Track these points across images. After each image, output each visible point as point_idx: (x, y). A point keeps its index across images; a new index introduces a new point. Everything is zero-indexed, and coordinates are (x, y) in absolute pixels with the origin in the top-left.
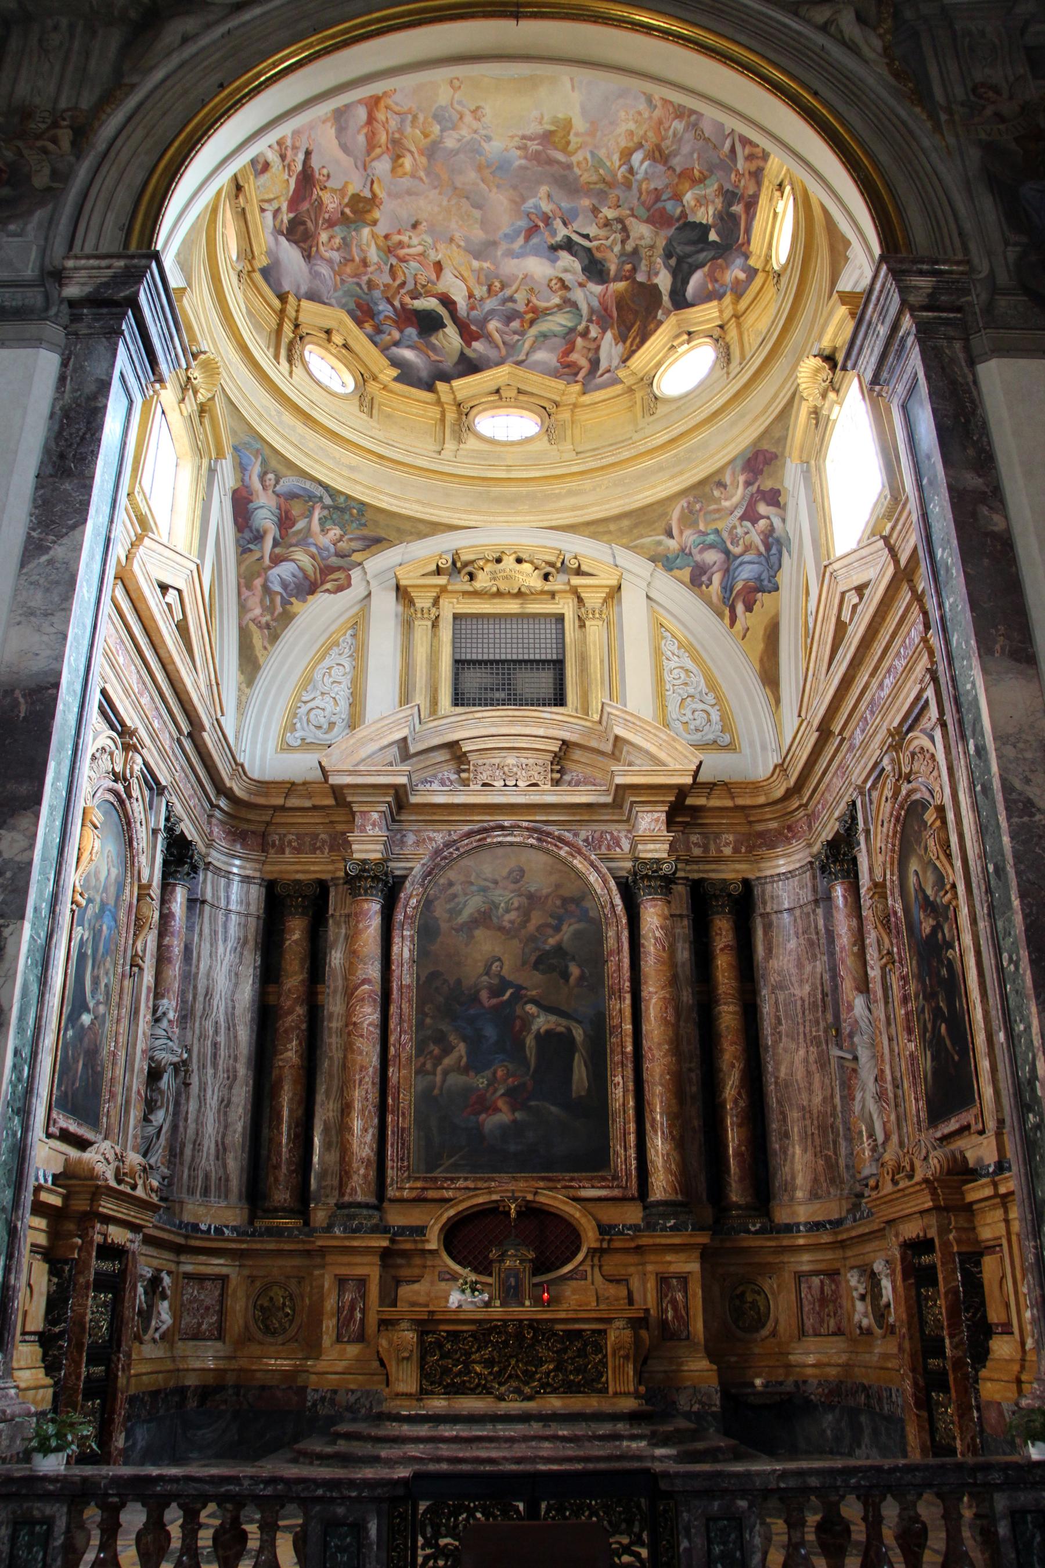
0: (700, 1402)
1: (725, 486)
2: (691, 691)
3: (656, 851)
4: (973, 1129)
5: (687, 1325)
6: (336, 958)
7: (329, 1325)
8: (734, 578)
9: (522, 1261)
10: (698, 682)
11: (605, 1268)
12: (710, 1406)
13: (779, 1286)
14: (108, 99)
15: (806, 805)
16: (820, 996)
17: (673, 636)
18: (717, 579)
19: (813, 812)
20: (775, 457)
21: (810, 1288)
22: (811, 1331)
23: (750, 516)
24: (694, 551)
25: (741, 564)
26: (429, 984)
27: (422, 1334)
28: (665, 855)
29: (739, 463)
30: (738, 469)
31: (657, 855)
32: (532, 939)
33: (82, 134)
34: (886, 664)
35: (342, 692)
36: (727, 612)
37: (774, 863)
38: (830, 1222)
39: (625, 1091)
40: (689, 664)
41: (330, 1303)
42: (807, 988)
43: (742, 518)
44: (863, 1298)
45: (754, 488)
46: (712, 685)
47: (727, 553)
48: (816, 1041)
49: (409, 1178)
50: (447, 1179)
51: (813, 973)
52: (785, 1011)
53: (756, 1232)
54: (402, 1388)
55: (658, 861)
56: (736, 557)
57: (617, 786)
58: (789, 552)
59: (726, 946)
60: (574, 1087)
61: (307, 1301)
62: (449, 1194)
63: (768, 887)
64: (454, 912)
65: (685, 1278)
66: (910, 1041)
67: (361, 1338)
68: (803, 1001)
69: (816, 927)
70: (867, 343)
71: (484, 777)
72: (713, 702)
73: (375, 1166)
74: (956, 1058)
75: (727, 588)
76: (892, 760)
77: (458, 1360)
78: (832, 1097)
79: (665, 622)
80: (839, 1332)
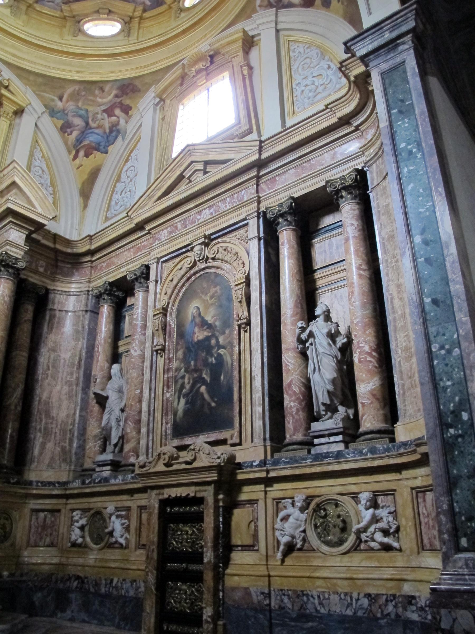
1: (103, 91)
2: (42, 181)
3: (16, 253)
4: (229, 442)
8: (85, 138)
10: (47, 179)
13: (20, 517)
15: (92, 262)
16: (77, 360)
17: (41, 150)
18: (75, 134)
19: (96, 266)
20: (139, 91)
21: (37, 519)
22: (33, 544)
23: (109, 112)
24: (70, 114)
25: (92, 133)
28: (20, 257)
29: (118, 84)
30: (115, 87)
31: (16, 256)
34: (210, 203)
36: (74, 152)
37: (68, 285)
38: (59, 483)
42: (69, 354)
43: (104, 111)
44: (82, 528)
45: (119, 100)
46: (53, 184)
47: (87, 123)
48: (69, 384)
51: (75, 347)
52: (53, 364)
53: (14, 484)
55: (17, 259)
56: (91, 128)
57: (8, 208)
58: (123, 139)
59: (28, 320)
63: (58, 296)
66: (167, 392)
68: (65, 361)
69: (83, 324)
70: (370, 37)
72: (52, 192)
74: (213, 404)
75: (79, 141)
76: (202, 249)
78: (74, 414)
79: (39, 141)
80: (52, 545)
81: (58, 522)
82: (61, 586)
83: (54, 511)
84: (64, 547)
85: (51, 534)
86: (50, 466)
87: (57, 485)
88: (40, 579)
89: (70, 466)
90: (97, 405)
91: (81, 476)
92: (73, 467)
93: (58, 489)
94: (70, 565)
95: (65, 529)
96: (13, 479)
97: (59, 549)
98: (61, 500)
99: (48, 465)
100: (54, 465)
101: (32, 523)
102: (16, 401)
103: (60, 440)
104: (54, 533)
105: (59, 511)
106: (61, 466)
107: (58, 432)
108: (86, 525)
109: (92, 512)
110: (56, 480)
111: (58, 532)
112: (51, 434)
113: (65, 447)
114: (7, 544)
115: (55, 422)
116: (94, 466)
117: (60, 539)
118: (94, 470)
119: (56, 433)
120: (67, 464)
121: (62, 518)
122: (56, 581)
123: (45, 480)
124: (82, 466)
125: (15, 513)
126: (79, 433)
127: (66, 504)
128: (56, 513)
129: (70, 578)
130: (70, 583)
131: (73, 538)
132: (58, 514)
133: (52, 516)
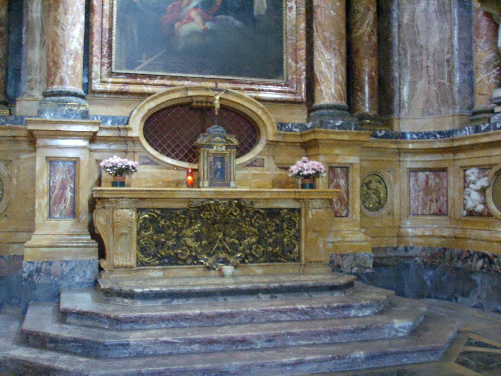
0: (358, 266)
5: (347, 205)
9: (228, 147)
11: (277, 158)
12: (366, 268)
13: (395, 178)
21: (417, 180)
27: (140, 210)
38: (440, 133)
39: (298, 14)
41: (42, 183)
44: (482, 191)
49: (111, 74)
50: (145, 76)
53: (382, 137)
54: (120, 261)
60: (256, 7)
61: (15, 182)
62: (149, 89)
65: (347, 168)
73: (81, 58)
77: (170, 234)
78: (451, 38)
80: (440, 213)
81: (445, 184)
82: (460, 264)
83: (439, 171)
84: (457, 217)
85: (437, 201)
86: (425, 112)
87: (438, 136)
88: (429, 254)
89: (454, 109)
90: (485, 18)
91: (472, 120)
92: (457, 111)
93: (440, 141)
94: (469, 239)
95: (457, 194)
96: (380, 132)
97: (450, 218)
98: (446, 155)
99: (423, 111)
100: (431, 110)
101: (411, 185)
102: (369, 29)
103: (434, 76)
104: (442, 198)
105: (444, 170)
106: (440, 111)
107: (431, 65)
108: (487, 187)
109: (495, 169)
110: (437, 130)
111: (447, 197)
112: (422, 70)
113: (444, 84)
114: (384, 211)
115: (424, 52)
116: (490, 106)
117: (450, 207)
118: (492, 111)
119: (428, 67)
120: (449, 107)
121: (451, 179)
122: (452, 259)
123: (422, 131)
124: (471, 107)
125: (388, 174)
126: (461, 64)
127: (454, 160)
128: (441, 173)
129: (471, 256)
130: (472, 261)
131: (470, 204)
132: (445, 174)
133: (438, 176)
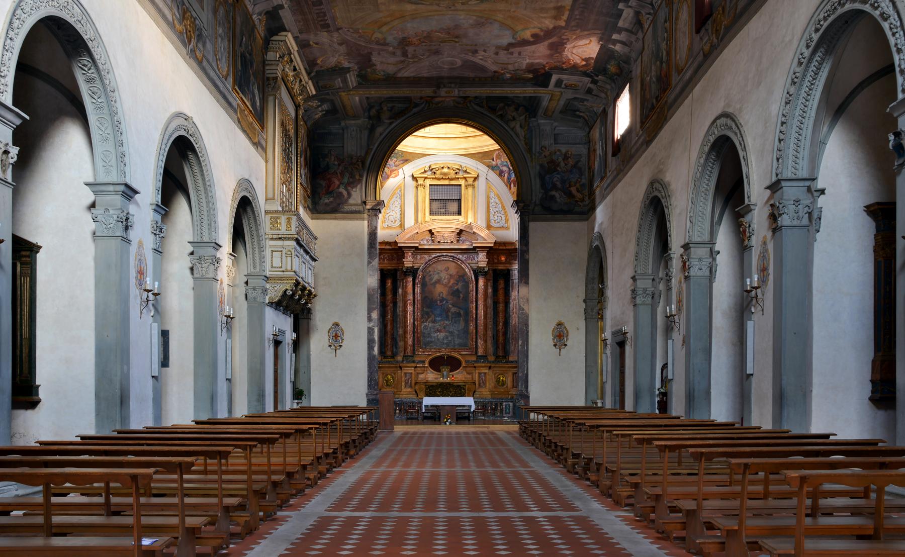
6: (400, 291)
7: (403, 384)
14: (367, 153)
26: (425, 299)
32: (451, 287)
33: (363, 163)
35: (398, 210)
40: (497, 201)
64: (431, 279)
67: (411, 386)
71: (438, 240)
